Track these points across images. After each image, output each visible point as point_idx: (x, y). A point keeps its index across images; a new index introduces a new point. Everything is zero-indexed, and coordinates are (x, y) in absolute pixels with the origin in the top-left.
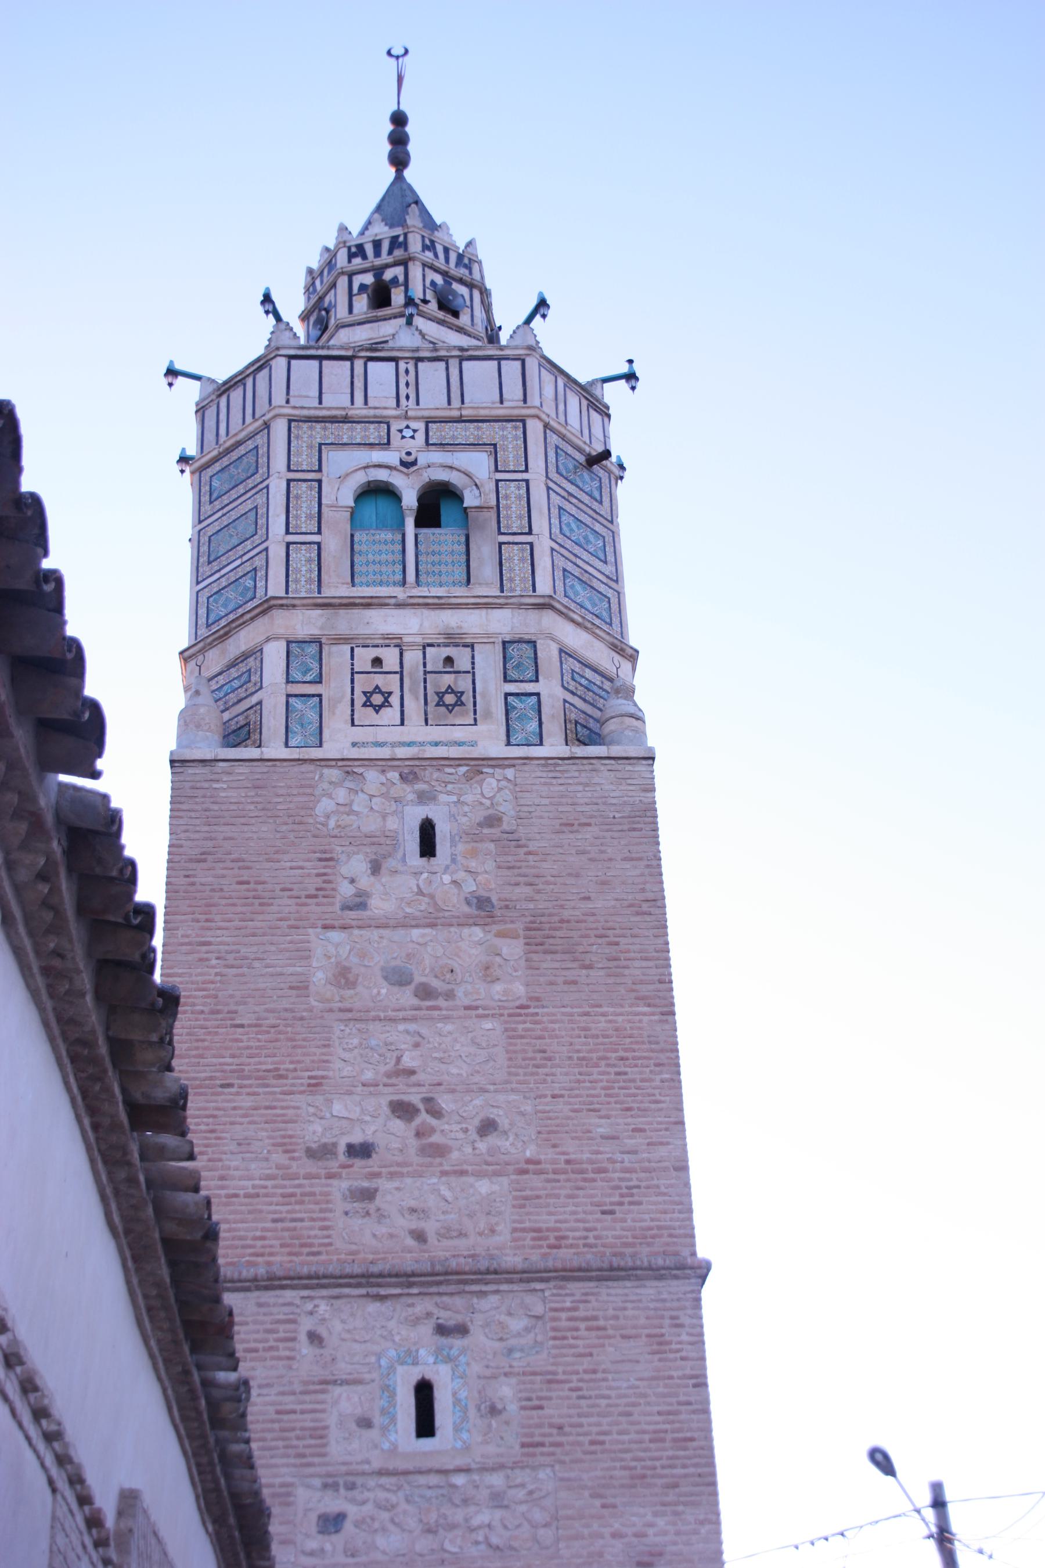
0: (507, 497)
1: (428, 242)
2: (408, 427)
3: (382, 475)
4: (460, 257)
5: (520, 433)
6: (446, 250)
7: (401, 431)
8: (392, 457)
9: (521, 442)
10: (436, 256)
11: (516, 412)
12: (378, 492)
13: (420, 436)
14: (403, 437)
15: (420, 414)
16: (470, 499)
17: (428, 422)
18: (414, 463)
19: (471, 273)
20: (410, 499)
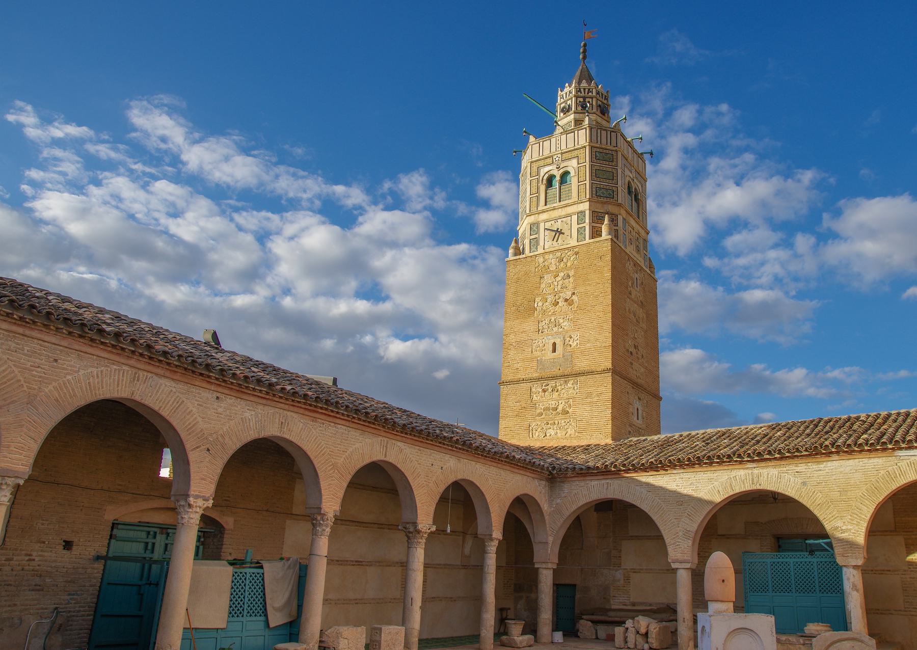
3: (551, 173)
8: (553, 167)
16: (572, 174)
17: (562, 154)
20: (558, 178)
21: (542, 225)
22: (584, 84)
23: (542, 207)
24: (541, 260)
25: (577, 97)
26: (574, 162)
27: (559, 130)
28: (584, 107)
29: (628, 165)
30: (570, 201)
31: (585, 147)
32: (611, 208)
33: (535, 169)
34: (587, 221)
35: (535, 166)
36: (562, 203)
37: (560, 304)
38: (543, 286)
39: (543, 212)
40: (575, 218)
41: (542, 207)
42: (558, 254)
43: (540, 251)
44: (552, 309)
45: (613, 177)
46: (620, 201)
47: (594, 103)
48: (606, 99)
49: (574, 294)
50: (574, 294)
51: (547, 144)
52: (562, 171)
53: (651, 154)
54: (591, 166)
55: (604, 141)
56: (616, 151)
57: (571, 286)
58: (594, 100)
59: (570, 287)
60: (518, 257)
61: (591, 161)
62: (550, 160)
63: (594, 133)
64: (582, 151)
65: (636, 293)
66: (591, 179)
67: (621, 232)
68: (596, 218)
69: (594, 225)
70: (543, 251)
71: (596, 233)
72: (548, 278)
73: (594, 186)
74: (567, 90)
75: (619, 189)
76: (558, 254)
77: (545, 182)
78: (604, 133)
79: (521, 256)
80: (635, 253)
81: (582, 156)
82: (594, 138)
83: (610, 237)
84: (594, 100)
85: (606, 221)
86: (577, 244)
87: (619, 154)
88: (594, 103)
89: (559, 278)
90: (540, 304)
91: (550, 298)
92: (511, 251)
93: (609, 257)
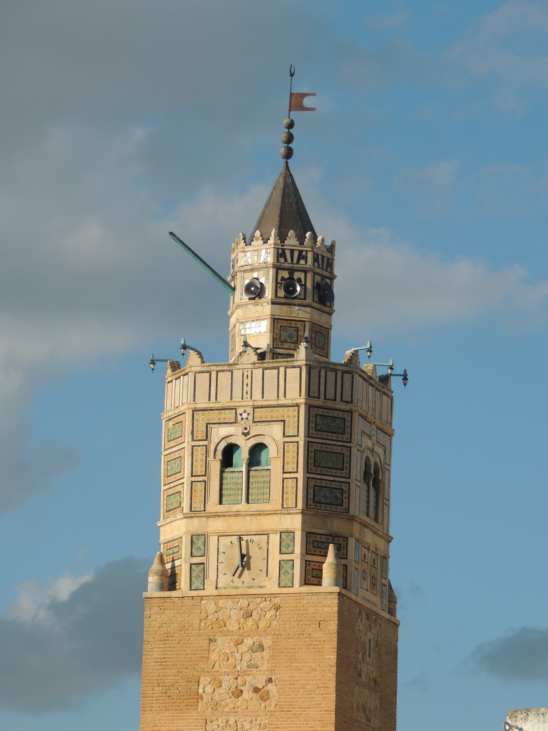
0: (288, 452)
1: (280, 251)
2: (245, 412)
4: (301, 252)
5: (296, 413)
6: (292, 251)
7: (241, 415)
9: (296, 419)
10: (286, 260)
11: (294, 402)
13: (251, 417)
14: (242, 419)
15: (251, 403)
16: (272, 452)
17: (255, 408)
18: (248, 433)
19: (306, 262)
21: (213, 540)
22: (291, 241)
23: (213, 505)
24: (211, 607)
25: (278, 268)
26: (277, 428)
30: (268, 507)
31: (297, 405)
32: (337, 525)
33: (200, 426)
34: (298, 550)
35: (202, 419)
36: (254, 507)
37: (245, 695)
38: (214, 656)
39: (217, 515)
40: (275, 539)
41: (213, 505)
42: (243, 602)
43: (210, 590)
44: (231, 701)
45: (342, 463)
46: (352, 512)
47: (309, 285)
48: (330, 264)
49: (270, 680)
50: (270, 680)
51: (224, 377)
52: (253, 442)
53: (405, 379)
54: (308, 445)
55: (330, 394)
56: (351, 412)
57: (265, 666)
58: (309, 275)
59: (264, 668)
60: (167, 594)
61: (308, 435)
62: (229, 416)
63: (315, 379)
64: (292, 412)
65: (368, 668)
66: (307, 470)
67: (351, 570)
68: (314, 544)
69: (309, 558)
70: (215, 592)
71: (312, 576)
72: (223, 644)
73: (311, 484)
75: (353, 487)
76: (243, 602)
77: (219, 456)
78: (331, 375)
79: (173, 594)
80: (369, 595)
81: (291, 422)
82: (314, 388)
83: (337, 589)
84: (309, 275)
85: (331, 557)
86: (279, 590)
87: (356, 416)
88: (309, 285)
89: (243, 648)
90: (209, 689)
91: (228, 682)
92: (153, 580)
93: (333, 626)
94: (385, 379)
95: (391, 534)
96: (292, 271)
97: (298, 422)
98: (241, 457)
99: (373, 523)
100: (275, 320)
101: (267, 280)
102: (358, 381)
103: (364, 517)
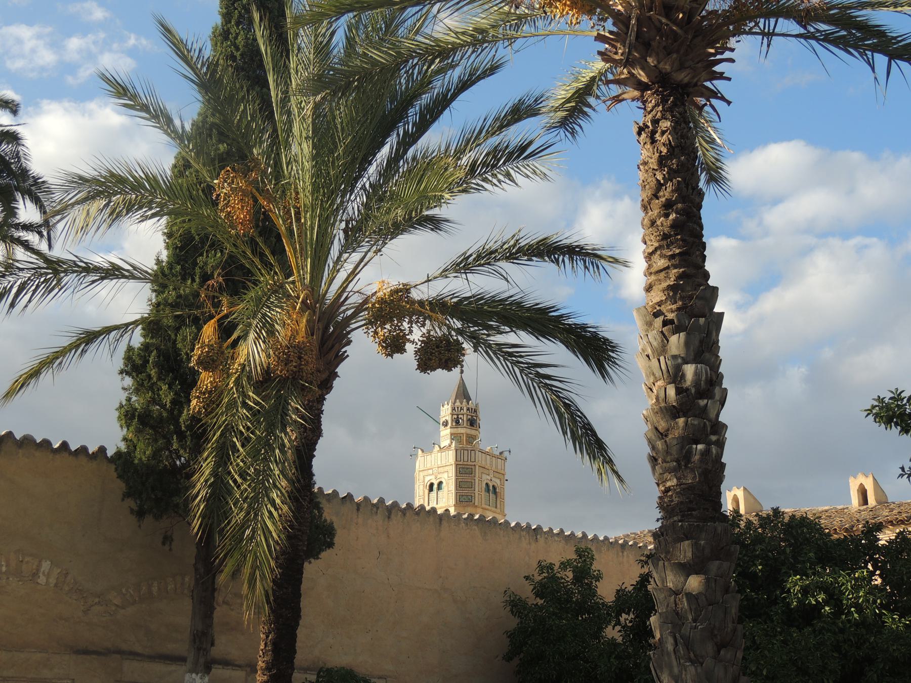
8: (432, 477)
12: (432, 485)
16: (444, 485)
22: (458, 404)
27: (437, 448)
28: (457, 422)
29: (486, 471)
45: (471, 486)
48: (475, 411)
51: (429, 457)
54: (456, 479)
55: (466, 459)
62: (430, 472)
66: (456, 489)
74: (446, 406)
78: (466, 452)
87: (477, 467)
94: (501, 453)
95: (506, 512)
96: (458, 415)
97: (452, 471)
98: (435, 486)
99: (494, 509)
100: (451, 434)
101: (449, 418)
102: (479, 454)
103: (484, 506)
